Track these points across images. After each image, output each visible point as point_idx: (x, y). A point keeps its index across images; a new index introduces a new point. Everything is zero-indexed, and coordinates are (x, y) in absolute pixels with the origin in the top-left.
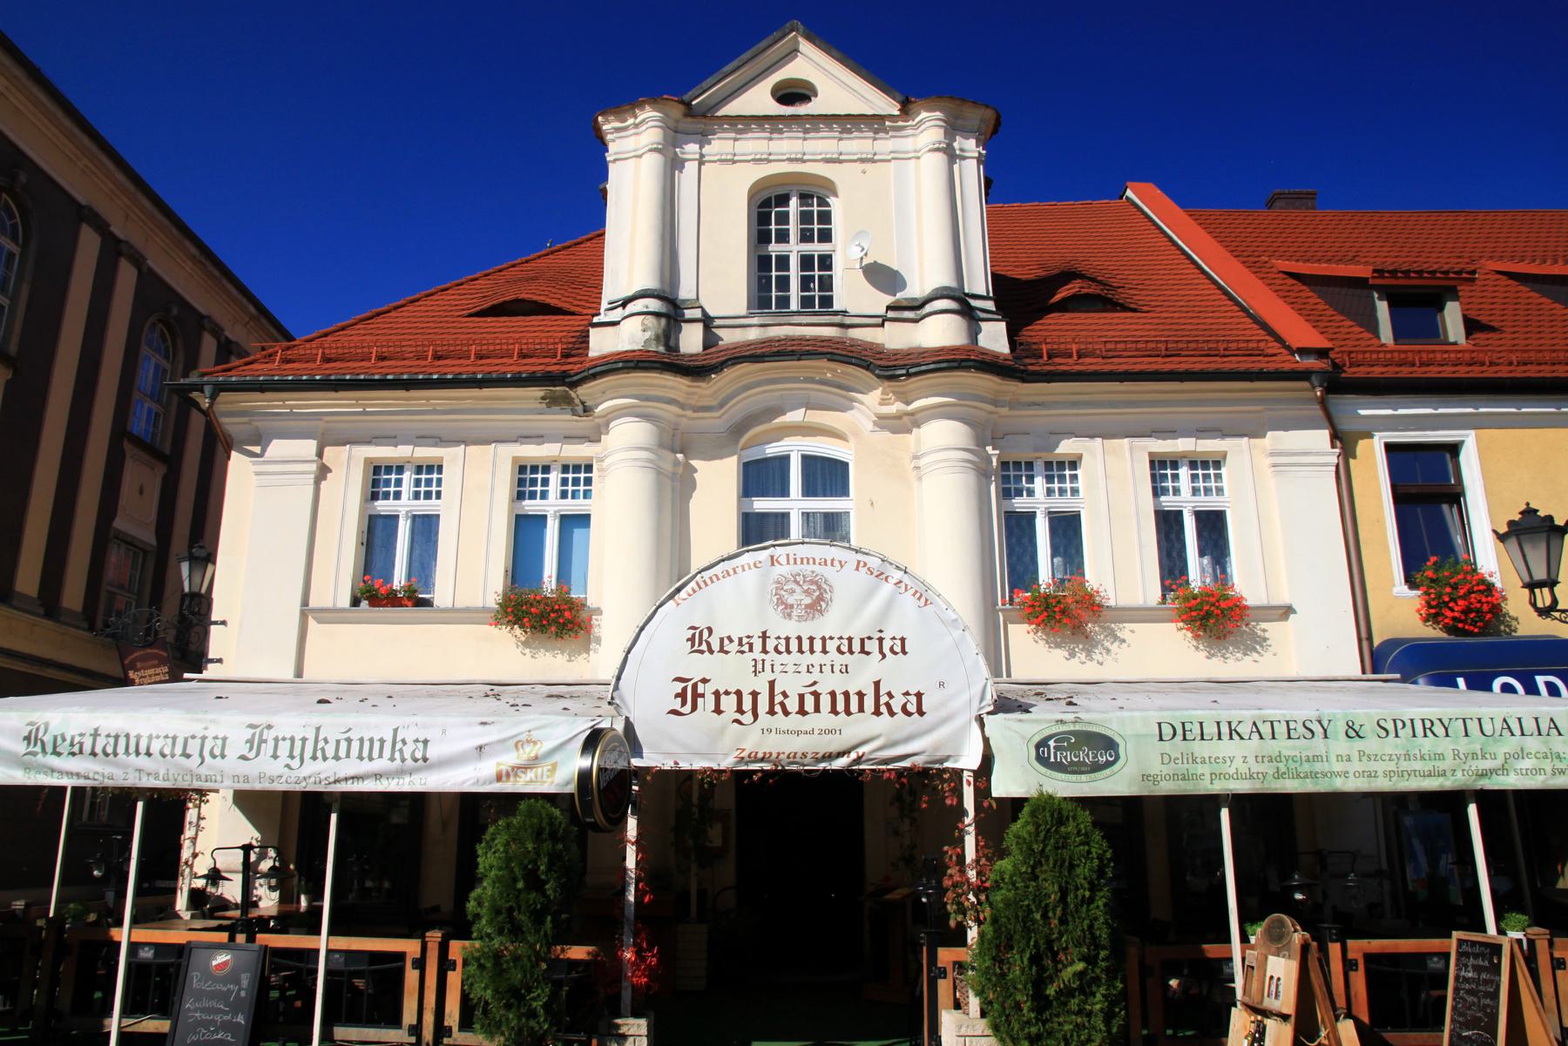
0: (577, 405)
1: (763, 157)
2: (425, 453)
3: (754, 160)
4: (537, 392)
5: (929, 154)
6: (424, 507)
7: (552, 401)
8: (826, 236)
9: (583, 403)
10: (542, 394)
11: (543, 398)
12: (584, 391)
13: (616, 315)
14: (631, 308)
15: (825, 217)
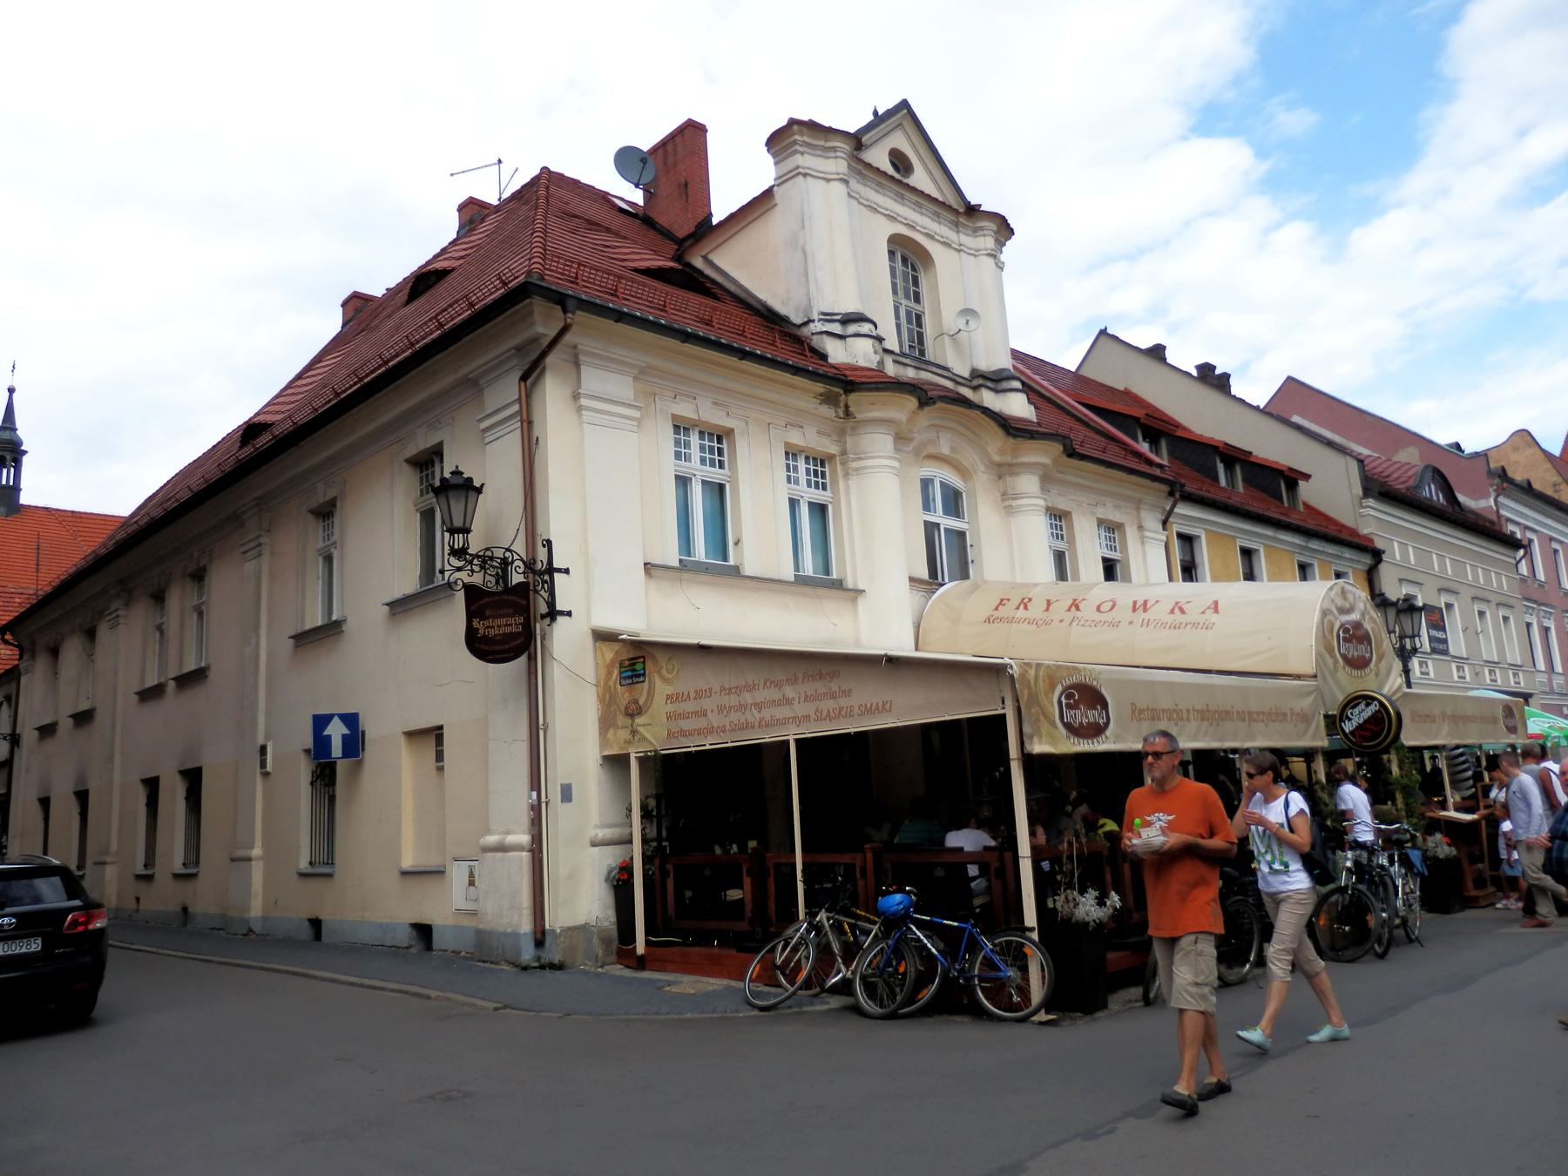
0: (841, 407)
1: (895, 216)
2: (718, 418)
3: (888, 215)
4: (819, 387)
5: (985, 257)
6: (716, 475)
7: (828, 399)
8: (917, 299)
9: (847, 406)
10: (822, 390)
11: (821, 395)
12: (853, 398)
13: (836, 328)
14: (852, 328)
15: (916, 282)
